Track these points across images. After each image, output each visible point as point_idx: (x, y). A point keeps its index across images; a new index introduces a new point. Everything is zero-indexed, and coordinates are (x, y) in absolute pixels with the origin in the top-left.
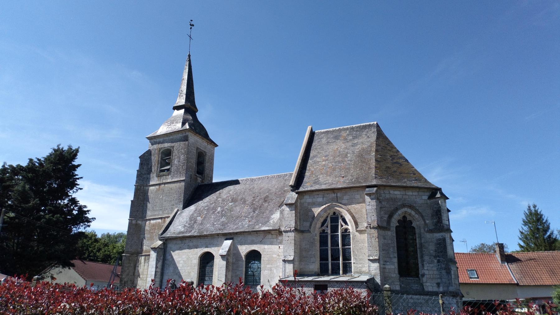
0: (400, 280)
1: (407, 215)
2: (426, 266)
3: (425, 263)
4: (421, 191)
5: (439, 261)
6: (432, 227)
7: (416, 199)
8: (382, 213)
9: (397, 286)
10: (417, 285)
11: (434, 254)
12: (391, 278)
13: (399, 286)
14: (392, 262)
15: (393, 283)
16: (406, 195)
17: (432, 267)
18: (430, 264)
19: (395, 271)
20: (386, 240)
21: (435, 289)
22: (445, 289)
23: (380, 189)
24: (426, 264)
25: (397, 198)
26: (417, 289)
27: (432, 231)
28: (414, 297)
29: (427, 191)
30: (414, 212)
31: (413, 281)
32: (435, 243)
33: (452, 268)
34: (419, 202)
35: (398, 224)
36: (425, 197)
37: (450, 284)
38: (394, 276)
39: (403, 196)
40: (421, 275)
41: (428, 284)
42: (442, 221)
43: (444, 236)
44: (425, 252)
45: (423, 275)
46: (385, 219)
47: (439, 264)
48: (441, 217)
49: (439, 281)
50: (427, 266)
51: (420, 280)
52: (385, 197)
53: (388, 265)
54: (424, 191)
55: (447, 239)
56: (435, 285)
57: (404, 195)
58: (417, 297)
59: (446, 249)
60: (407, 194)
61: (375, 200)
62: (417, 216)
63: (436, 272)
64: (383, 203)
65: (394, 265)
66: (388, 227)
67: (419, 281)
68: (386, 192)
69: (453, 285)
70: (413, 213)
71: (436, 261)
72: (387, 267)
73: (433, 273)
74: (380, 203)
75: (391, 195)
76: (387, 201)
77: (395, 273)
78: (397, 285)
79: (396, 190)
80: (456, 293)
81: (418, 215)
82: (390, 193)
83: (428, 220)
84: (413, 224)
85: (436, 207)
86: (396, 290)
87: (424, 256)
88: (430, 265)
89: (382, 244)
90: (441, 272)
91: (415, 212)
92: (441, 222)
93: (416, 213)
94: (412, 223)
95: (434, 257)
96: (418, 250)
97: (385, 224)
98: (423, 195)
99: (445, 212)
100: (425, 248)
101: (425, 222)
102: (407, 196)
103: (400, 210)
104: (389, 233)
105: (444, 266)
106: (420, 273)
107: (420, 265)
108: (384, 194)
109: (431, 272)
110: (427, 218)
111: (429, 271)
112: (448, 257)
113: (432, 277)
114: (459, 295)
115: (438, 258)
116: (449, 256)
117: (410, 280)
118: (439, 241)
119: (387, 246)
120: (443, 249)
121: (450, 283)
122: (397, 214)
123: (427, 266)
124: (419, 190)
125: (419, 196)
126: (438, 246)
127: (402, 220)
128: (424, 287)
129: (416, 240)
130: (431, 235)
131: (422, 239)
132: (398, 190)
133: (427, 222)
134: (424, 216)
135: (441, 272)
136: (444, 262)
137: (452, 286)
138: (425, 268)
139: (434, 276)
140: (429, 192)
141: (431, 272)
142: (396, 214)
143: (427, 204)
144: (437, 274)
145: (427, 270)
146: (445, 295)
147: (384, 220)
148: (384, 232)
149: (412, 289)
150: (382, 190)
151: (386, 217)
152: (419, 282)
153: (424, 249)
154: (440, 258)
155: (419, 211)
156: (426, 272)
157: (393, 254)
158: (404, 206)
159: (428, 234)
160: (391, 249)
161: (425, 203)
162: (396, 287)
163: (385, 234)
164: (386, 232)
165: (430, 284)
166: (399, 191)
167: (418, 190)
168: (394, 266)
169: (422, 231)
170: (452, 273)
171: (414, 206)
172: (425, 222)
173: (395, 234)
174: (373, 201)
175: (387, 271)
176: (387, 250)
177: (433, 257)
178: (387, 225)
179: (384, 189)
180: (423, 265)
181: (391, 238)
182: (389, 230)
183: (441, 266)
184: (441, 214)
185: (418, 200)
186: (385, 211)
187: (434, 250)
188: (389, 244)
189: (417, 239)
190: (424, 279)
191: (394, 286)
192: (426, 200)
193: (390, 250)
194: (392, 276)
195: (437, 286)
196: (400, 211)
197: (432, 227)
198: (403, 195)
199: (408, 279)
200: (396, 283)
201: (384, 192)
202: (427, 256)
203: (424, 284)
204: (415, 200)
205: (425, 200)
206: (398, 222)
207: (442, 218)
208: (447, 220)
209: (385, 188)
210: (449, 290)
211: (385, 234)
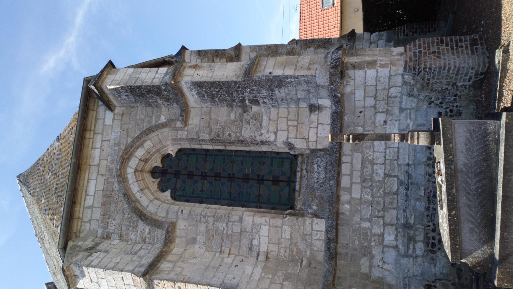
0: (302, 215)
1: (149, 166)
2: (267, 136)
3: (258, 138)
4: (95, 126)
5: (255, 102)
6: (176, 110)
7: (111, 142)
8: (132, 236)
9: (316, 227)
10: (316, 165)
11: (240, 110)
12: (294, 241)
13: (316, 220)
14: (252, 229)
15: (307, 237)
16: (98, 165)
17: (270, 119)
18: (261, 125)
19: (276, 226)
20: (198, 237)
21: (326, 117)
22: (324, 93)
23: (80, 232)
24: (261, 134)
25: (103, 190)
26: (325, 169)
27: (184, 111)
28: (345, 181)
29: (95, 112)
30: (140, 150)
31: (304, 172)
32: (213, 105)
33: (267, 72)
34: (117, 134)
35: (168, 193)
36: (109, 115)
37: (309, 81)
38: (289, 230)
39: (100, 173)
40: (290, 149)
41: (313, 138)
42: (153, 86)
43: (188, 86)
44: (233, 135)
45: (290, 145)
46: (147, 230)
47: (261, 102)
48: (145, 86)
49: (304, 105)
51: (302, 155)
52: (98, 220)
53: (260, 243)
54: (96, 119)
55: (197, 79)
56: (314, 117)
57: (99, 171)
58: (345, 169)
59: (219, 82)
60: (96, 162)
61: (82, 268)
62: (148, 144)
63: (283, 111)
64: (111, 229)
65: (260, 225)
66: (167, 226)
67: (304, 156)
68: (87, 215)
69: (311, 72)
70: (140, 153)
71: (255, 108)
72: (264, 248)
73: (285, 120)
74: (110, 238)
75: (96, 205)
76: (107, 216)
77: (281, 227)
78: (312, 224)
79: (86, 191)
80: (333, 67)
81: (145, 141)
82: (91, 207)
83: (159, 117)
84: (170, 152)
85: (126, 96)
86: (327, 232)
87: (241, 138)
88: (264, 123)
89: (207, 250)
90: (282, 100)
91: (137, 148)
92: (158, 87)
93: (142, 145)
94: (169, 155)
95: (245, 112)
96: (229, 148)
97: (160, 234)
98: (104, 122)
99: (137, 76)
100: (223, 133)
101: (164, 125)
102: (102, 161)
103: (130, 189)
104: (181, 225)
105: (264, 91)
106: (287, 150)
107: (265, 148)
108: (92, 222)
109: (283, 125)
110: (154, 118)
111: (279, 129)
112: (240, 79)
113: (295, 123)
114: (339, 58)
115: (247, 102)
116: (238, 77)
117: (301, 181)
118: (204, 96)
119: (213, 236)
120: (221, 91)
121: (308, 82)
122: (138, 195)
124: (90, 130)
125: (104, 133)
126: (216, 99)
127: (159, 180)
128: (319, 147)
129: (207, 150)
130: (193, 113)
131: (201, 138)
132: (85, 184)
133: (163, 119)
134: (148, 127)
135: (282, 100)
136: (253, 90)
137: (315, 76)
138: (272, 138)
139: (291, 116)
140: (98, 106)
141: (283, 125)
142: (137, 201)
143: (123, 114)
144: (288, 108)
145: (276, 133)
146: (339, 95)
147: (149, 233)
148: (178, 240)
149: (323, 182)
150: (83, 228)
151: (144, 228)
152: (308, 157)
153: (226, 136)
154: (247, 98)
155: (137, 137)
156: (282, 137)
157: (233, 225)
158: (122, 177)
159: (190, 121)
160: (221, 226)
161: (122, 120)
162: (317, 231)
163: (181, 237)
164: (178, 232)
165: (313, 132)
166: (88, 183)
167: (92, 133)
168: (262, 226)
169: (182, 134)
170: (278, 72)
171: (126, 149)
172: (164, 125)
173: (187, 207)
174: (86, 274)
175: (274, 248)
176: (222, 238)
177: (245, 114)
178: (162, 229)
179: (80, 221)
180: (263, 143)
181: (194, 223)
182: (173, 225)
183: (266, 98)
184: (140, 87)
185: (113, 137)
186: (130, 228)
187: (230, 108)
188: (207, 231)
189: (205, 147)
190: (300, 145)
191: (316, 238)
192: (115, 114)
193: (223, 231)
194: (287, 235)
195: (317, 112)
196: (132, 186)
197: (176, 110)
198: (98, 174)
199: (300, 188)
200: (308, 228)
201: (86, 222)
202: (241, 129)
203: (312, 146)
204: (112, 142)
205: (114, 119)
206: (163, 191)
207: (147, 84)
208: (157, 72)
209: (79, 218)
210: (327, 84)
211: (181, 237)
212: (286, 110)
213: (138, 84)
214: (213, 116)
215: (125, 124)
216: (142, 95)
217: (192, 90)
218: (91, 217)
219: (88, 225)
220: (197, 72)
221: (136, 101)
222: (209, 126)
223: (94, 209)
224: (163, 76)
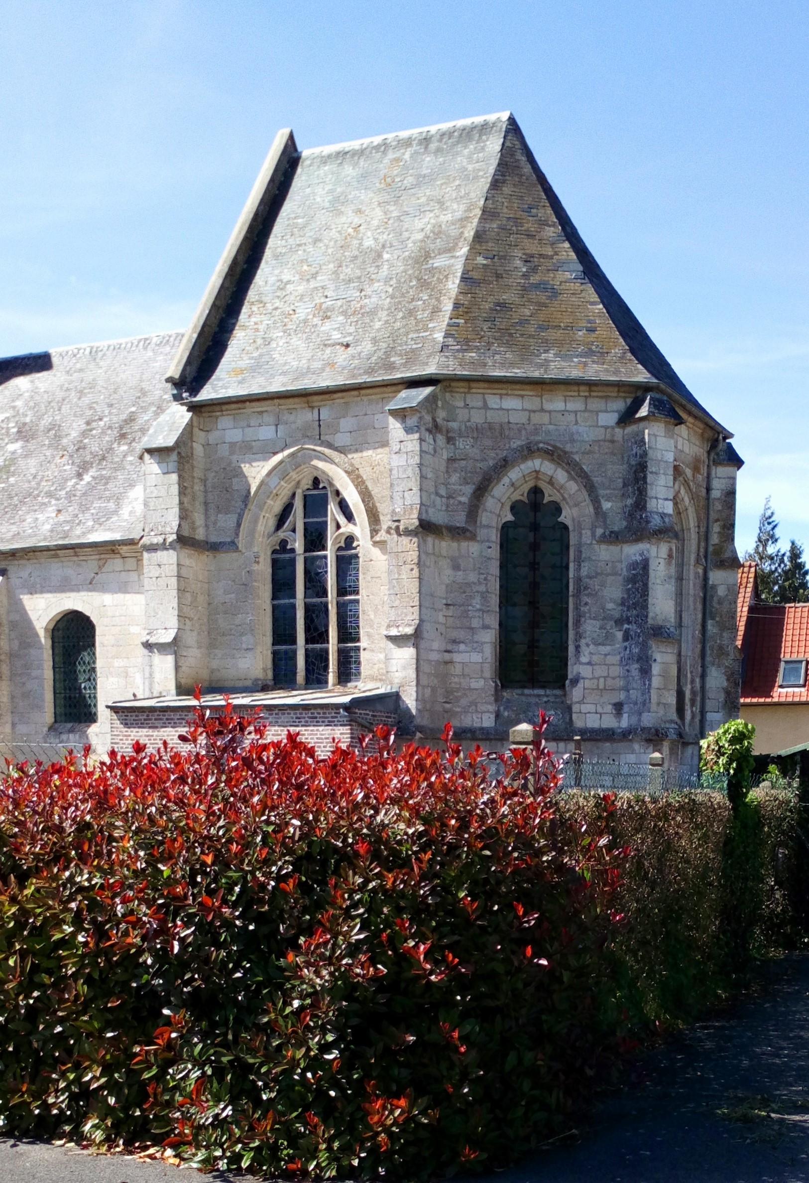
8: (455, 478)
11: (617, 615)
18: (600, 644)
21: (609, 722)
24: (588, 645)
36: (610, 419)
39: (532, 415)
41: (585, 708)
43: (645, 552)
48: (646, 489)
50: (591, 653)
55: (653, 565)
57: (534, 411)
70: (561, 476)
79: (507, 394)
83: (608, 499)
95: (616, 622)
96: (571, 600)
99: (662, 472)
108: (467, 411)
118: (634, 569)
123: (591, 653)
125: (586, 414)
126: (630, 586)
129: (567, 568)
208: (666, 499)
212: (617, 674)
213: (650, 478)
214: (610, 579)
215: (600, 446)
216: (637, 480)
217: (641, 555)
218: (473, 408)
219: (462, 404)
220: (662, 561)
221: (631, 466)
222: (597, 574)
223: (484, 411)
224: (660, 511)
